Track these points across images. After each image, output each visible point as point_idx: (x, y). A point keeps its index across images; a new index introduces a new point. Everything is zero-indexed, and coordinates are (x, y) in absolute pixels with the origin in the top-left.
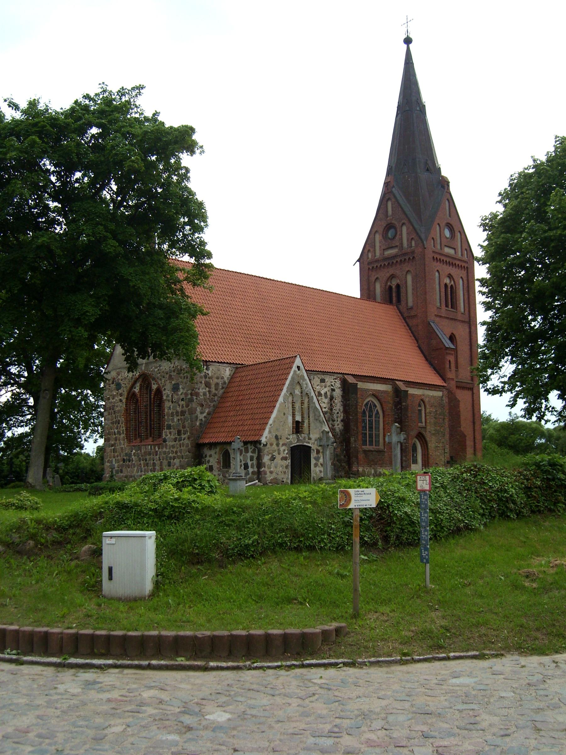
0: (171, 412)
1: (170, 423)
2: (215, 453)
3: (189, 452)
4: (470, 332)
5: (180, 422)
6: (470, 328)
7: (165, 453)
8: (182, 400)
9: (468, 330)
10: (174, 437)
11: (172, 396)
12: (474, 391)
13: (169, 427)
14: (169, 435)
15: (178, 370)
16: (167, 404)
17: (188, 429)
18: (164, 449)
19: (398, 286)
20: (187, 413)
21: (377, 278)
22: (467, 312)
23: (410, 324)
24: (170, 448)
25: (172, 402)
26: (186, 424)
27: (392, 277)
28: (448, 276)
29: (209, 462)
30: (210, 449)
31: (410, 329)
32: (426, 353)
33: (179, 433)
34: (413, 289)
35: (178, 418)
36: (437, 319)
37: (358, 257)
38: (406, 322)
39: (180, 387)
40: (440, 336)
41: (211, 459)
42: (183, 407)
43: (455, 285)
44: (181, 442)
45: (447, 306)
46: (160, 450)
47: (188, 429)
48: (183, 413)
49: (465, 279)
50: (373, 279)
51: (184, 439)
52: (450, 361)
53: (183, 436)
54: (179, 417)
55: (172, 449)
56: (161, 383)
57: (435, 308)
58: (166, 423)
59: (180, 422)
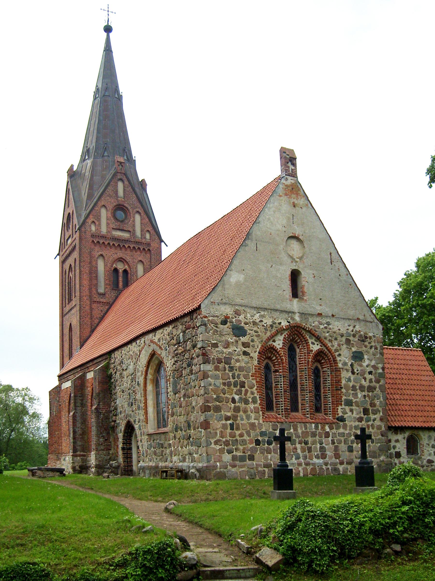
0: (351, 384)
1: (351, 397)
2: (404, 438)
3: (382, 435)
5: (367, 399)
7: (343, 435)
8: (370, 373)
10: (358, 416)
11: (352, 365)
13: (349, 403)
14: (350, 414)
15: (361, 336)
16: (345, 375)
17: (380, 409)
18: (341, 430)
20: (377, 389)
24: (351, 430)
25: (353, 373)
26: (377, 402)
29: (394, 447)
30: (396, 433)
33: (366, 411)
35: (363, 393)
39: (366, 357)
41: (398, 445)
42: (371, 381)
44: (370, 423)
46: (334, 431)
47: (380, 409)
48: (371, 389)
51: (374, 420)
53: (372, 417)
54: (366, 393)
55: (354, 430)
56: (333, 346)
58: (344, 398)
59: (367, 399)
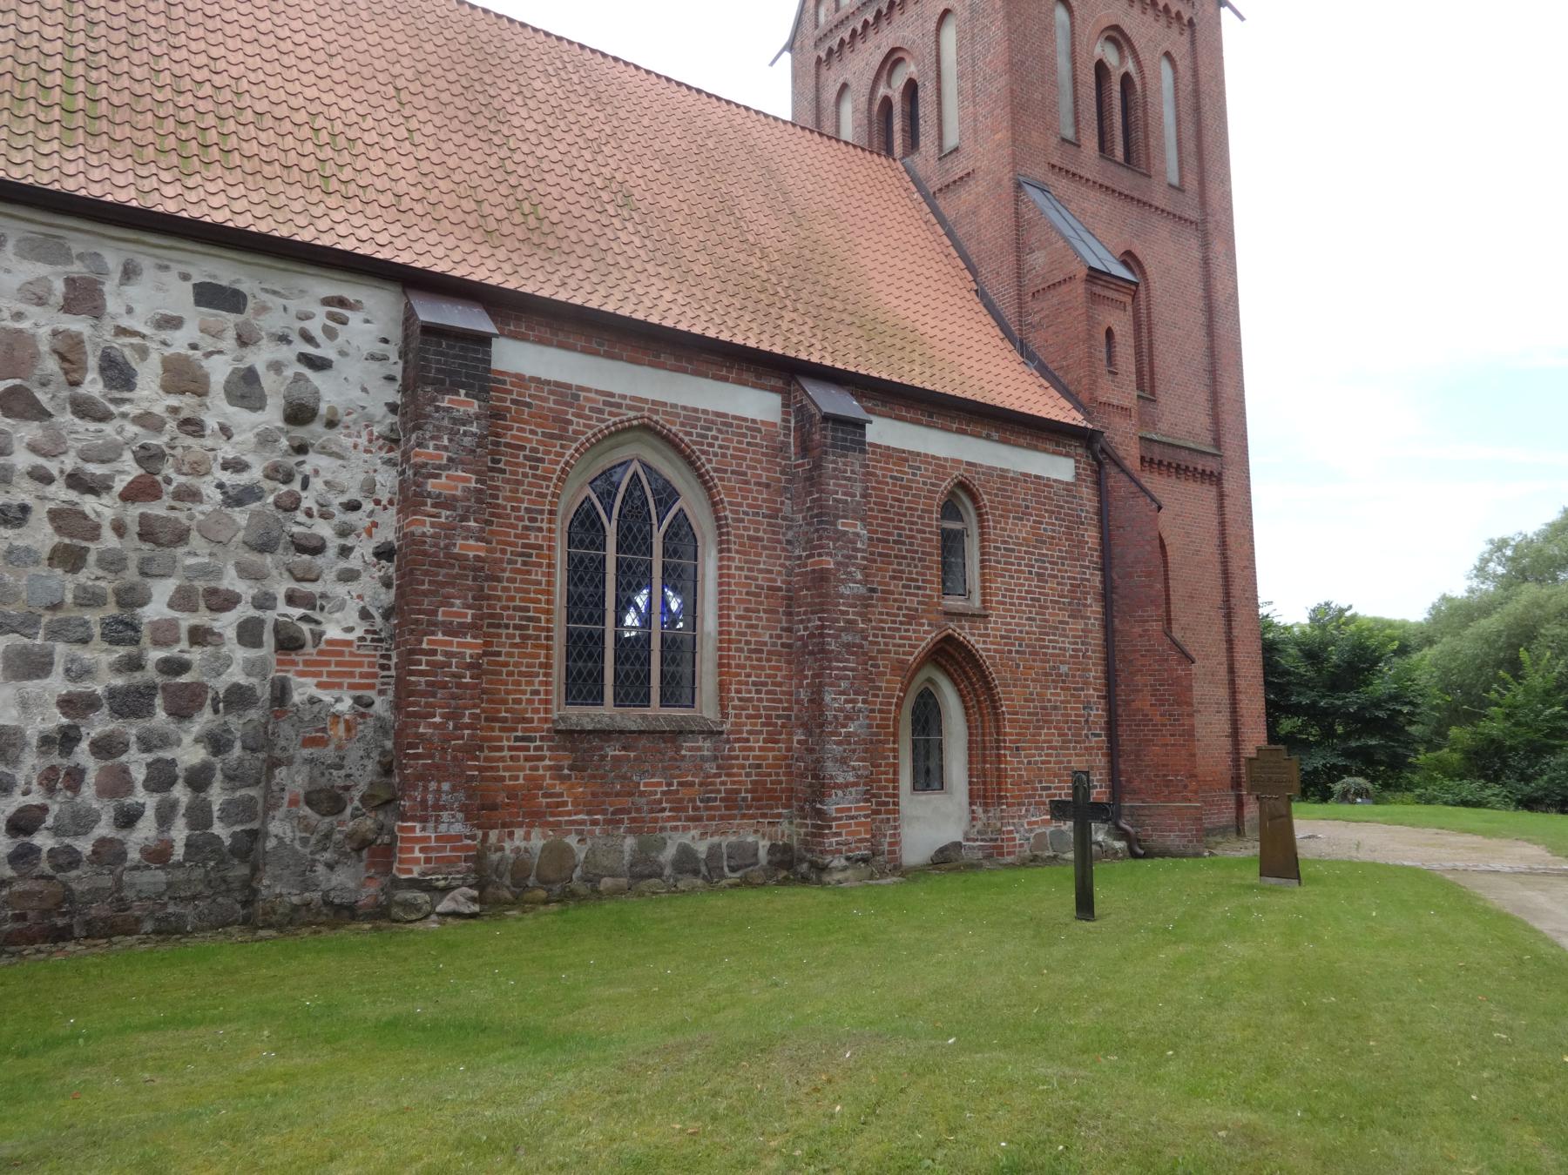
4: (1206, 262)
6: (1205, 245)
9: (1196, 254)
12: (1229, 485)
19: (911, 88)
21: (845, 86)
22: (1192, 183)
23: (950, 214)
27: (893, 60)
28: (1109, 39)
31: (950, 234)
32: (1010, 313)
34: (961, 76)
36: (1062, 185)
37: (785, 36)
38: (935, 211)
40: (1069, 232)
43: (1143, 78)
45: (1104, 146)
49: (1184, 64)
50: (830, 94)
52: (1109, 333)
57: (1054, 141)
